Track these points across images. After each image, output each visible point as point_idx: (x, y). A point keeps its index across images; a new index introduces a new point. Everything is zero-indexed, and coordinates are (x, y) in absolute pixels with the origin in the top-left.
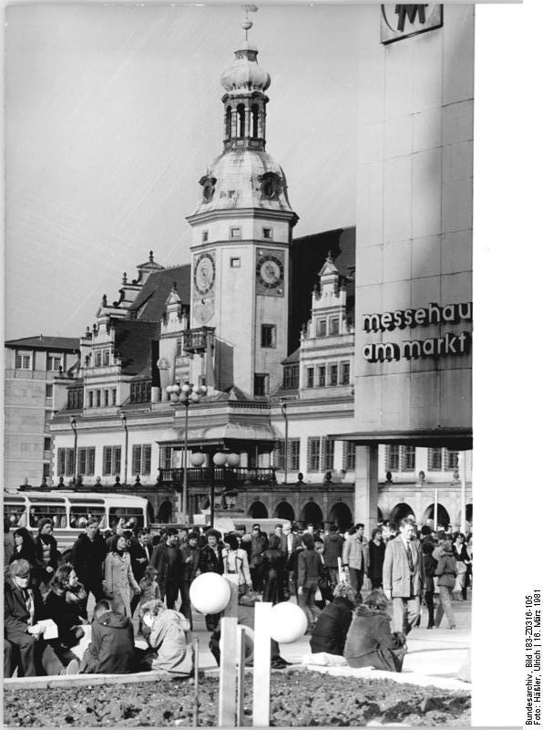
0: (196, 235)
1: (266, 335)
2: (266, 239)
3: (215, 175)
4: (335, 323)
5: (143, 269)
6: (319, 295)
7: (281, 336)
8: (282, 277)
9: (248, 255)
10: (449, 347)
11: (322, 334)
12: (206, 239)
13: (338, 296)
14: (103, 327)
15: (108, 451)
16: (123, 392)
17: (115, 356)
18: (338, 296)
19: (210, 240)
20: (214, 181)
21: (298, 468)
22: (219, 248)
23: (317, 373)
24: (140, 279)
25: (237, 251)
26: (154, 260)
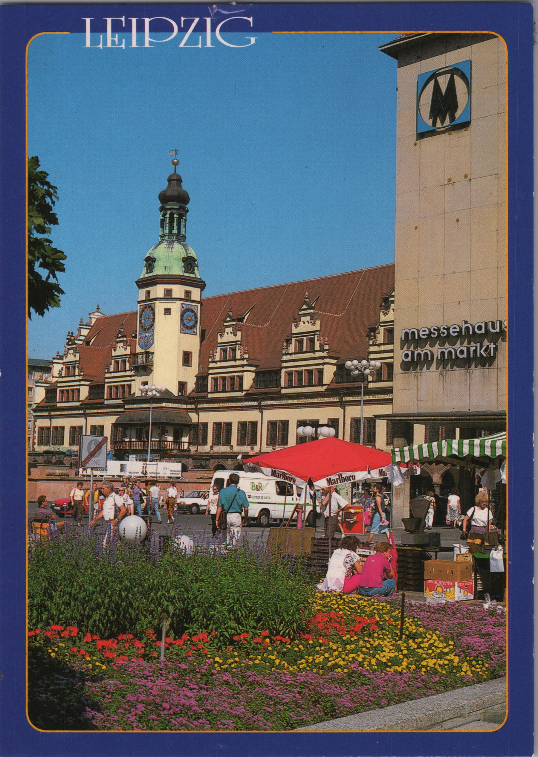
0: (142, 294)
1: (187, 358)
2: (187, 298)
3: (155, 256)
7: (195, 359)
8: (196, 322)
9: (176, 307)
10: (480, 353)
12: (149, 296)
15: (73, 428)
20: (154, 260)
21: (230, 443)
22: (157, 302)
23: (220, 382)
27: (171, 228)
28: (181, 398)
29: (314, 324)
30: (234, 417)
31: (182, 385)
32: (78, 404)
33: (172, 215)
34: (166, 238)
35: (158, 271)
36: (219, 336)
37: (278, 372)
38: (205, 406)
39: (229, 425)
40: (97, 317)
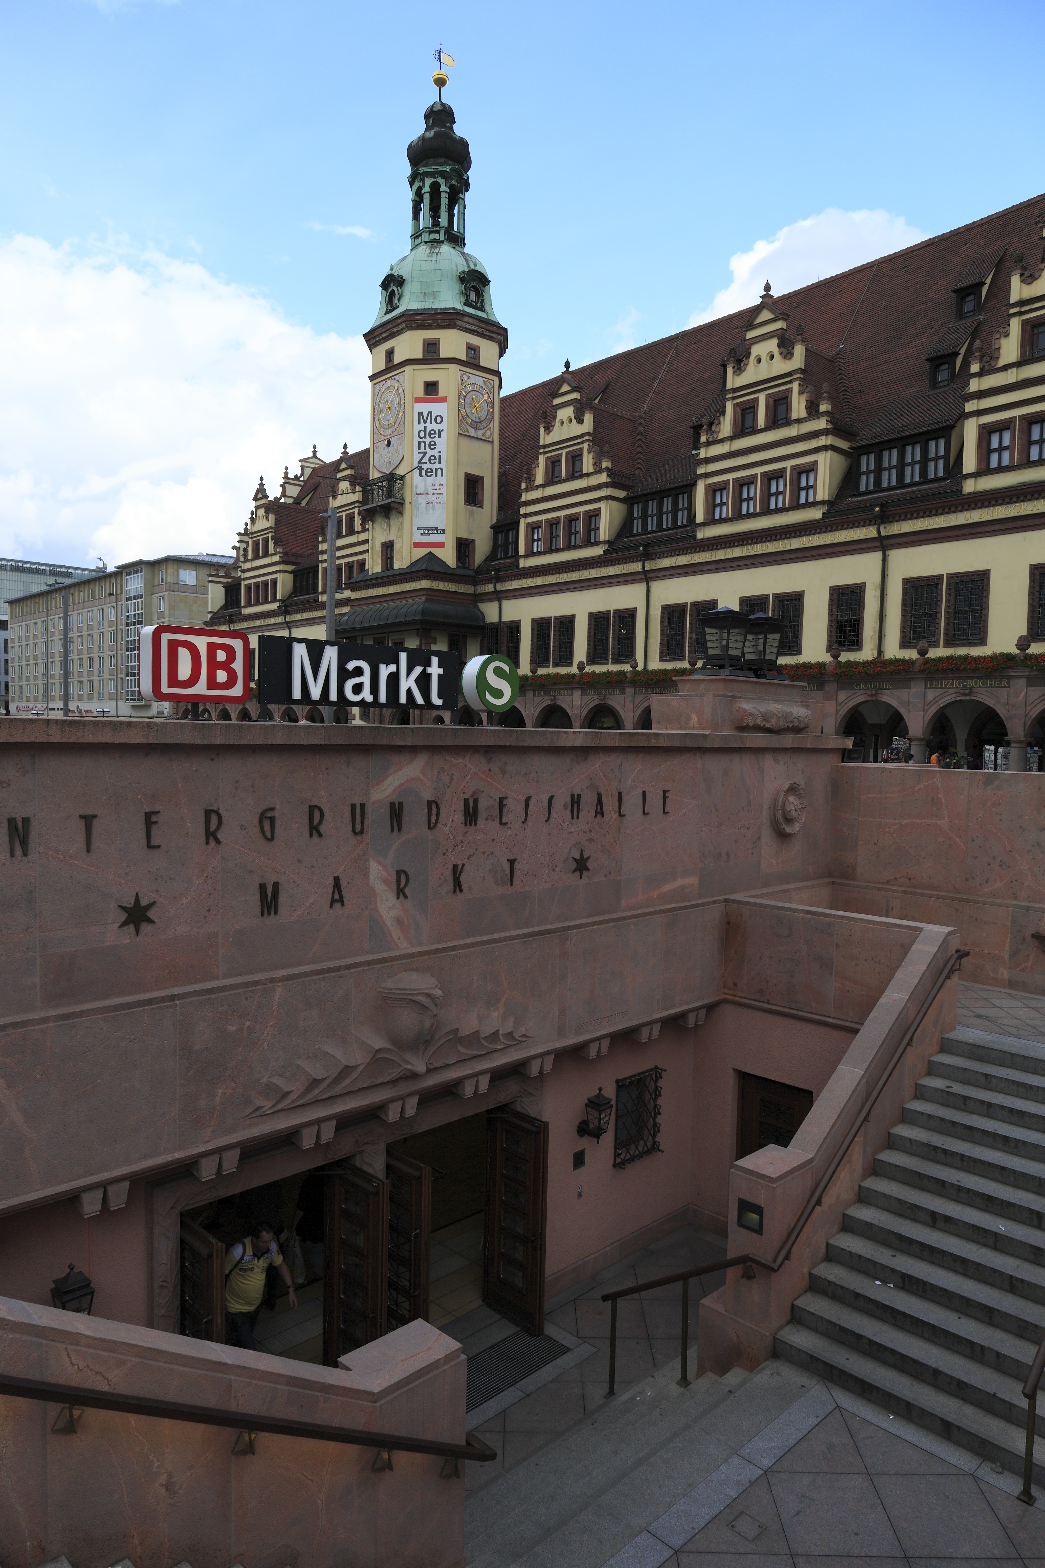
1: (473, 488)
2: (472, 361)
4: (576, 458)
5: (305, 464)
6: (548, 429)
11: (552, 479)
13: (580, 421)
14: (261, 512)
16: (284, 583)
17: (276, 543)
18: (580, 421)
19: (397, 360)
22: (408, 369)
24: (303, 474)
25: (431, 373)
26: (318, 455)
27: (436, 223)
28: (462, 572)
29: (787, 354)
30: (580, 605)
31: (464, 547)
32: (274, 606)
33: (435, 187)
34: (425, 237)
35: (409, 302)
36: (542, 430)
37: (689, 488)
38: (514, 585)
39: (567, 624)
40: (313, 466)
